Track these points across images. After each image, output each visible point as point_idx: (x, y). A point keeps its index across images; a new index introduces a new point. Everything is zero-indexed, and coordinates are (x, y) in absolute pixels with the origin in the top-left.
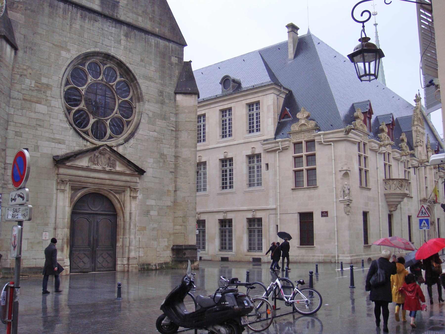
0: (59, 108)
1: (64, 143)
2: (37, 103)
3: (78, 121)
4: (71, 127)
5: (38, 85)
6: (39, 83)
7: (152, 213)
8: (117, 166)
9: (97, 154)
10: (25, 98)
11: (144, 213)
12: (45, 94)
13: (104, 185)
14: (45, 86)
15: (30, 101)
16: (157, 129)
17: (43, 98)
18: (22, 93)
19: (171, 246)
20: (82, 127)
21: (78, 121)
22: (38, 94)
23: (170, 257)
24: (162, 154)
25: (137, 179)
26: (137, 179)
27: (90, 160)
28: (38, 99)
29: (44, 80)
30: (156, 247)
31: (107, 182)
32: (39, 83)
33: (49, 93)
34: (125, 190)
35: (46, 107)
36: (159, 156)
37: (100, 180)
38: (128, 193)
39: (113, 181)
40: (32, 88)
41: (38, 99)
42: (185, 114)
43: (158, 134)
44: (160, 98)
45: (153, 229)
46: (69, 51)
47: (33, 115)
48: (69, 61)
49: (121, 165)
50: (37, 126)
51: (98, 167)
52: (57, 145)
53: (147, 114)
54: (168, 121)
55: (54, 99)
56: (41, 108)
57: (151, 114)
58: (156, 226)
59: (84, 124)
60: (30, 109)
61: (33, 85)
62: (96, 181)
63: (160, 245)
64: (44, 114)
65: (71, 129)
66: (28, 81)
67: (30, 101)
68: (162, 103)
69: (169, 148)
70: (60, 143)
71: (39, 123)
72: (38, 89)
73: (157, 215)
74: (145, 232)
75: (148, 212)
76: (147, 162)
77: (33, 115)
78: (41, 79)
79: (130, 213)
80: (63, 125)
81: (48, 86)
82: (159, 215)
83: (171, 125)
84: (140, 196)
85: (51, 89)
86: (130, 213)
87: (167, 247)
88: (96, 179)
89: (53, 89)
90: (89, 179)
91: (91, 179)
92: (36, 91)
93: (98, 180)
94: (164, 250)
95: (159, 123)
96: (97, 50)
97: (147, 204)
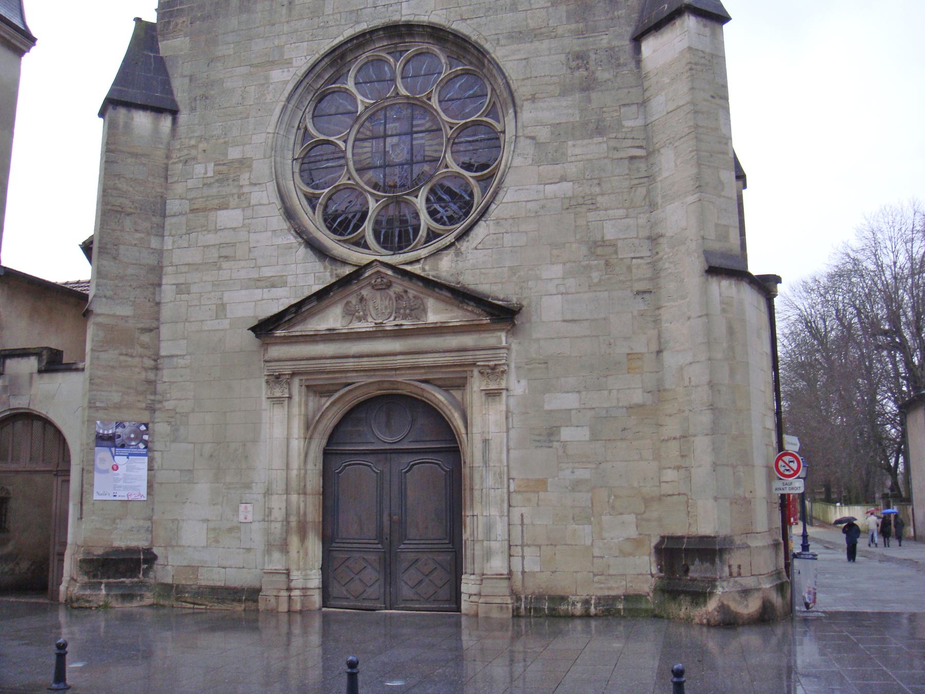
0: (269, 204)
1: (284, 284)
2: (220, 209)
3: (338, 220)
4: (300, 240)
5: (220, 168)
6: (224, 164)
7: (566, 434)
8: (429, 310)
9: (364, 292)
10: (195, 207)
11: (538, 438)
12: (236, 183)
13: (396, 369)
14: (236, 165)
15: (205, 210)
16: (572, 169)
17: (233, 195)
18: (188, 197)
19: (655, 541)
20: (349, 230)
21: (338, 220)
22: (220, 189)
23: (652, 575)
24: (595, 242)
25: (500, 337)
26: (502, 338)
27: (349, 313)
28: (221, 200)
29: (234, 154)
31: (400, 361)
32: (224, 164)
33: (244, 178)
34: (464, 375)
35: (238, 212)
36: (584, 250)
37: (376, 359)
38: (477, 384)
39: (416, 356)
40: (209, 181)
41: (221, 200)
42: (663, 93)
43: (576, 186)
44: (577, 74)
45: (576, 486)
46: (289, 63)
47: (211, 238)
48: (290, 87)
49: (441, 306)
50: (221, 259)
51: (365, 325)
52: (267, 293)
53: (528, 137)
54: (613, 135)
55: (256, 188)
56: (229, 218)
57: (543, 134)
58: (583, 474)
59: (354, 221)
60: (204, 228)
61: (210, 174)
63: (605, 535)
64: (234, 229)
65: (300, 244)
66: (199, 169)
67: (205, 210)
68: (588, 86)
69: (627, 217)
70: (273, 286)
71: (224, 252)
72: (221, 176)
73: (587, 438)
74: (542, 495)
75: (551, 434)
76: (538, 279)
77: (211, 238)
78: (226, 154)
79: (486, 442)
80: (279, 241)
81: (244, 163)
82: (594, 438)
83: (629, 143)
84: (517, 386)
85: (250, 166)
86: (486, 442)
87: (638, 543)
89: (255, 165)
92: (217, 185)
93: (370, 359)
94: (623, 554)
95: (578, 151)
96: (363, 27)
97: (547, 407)
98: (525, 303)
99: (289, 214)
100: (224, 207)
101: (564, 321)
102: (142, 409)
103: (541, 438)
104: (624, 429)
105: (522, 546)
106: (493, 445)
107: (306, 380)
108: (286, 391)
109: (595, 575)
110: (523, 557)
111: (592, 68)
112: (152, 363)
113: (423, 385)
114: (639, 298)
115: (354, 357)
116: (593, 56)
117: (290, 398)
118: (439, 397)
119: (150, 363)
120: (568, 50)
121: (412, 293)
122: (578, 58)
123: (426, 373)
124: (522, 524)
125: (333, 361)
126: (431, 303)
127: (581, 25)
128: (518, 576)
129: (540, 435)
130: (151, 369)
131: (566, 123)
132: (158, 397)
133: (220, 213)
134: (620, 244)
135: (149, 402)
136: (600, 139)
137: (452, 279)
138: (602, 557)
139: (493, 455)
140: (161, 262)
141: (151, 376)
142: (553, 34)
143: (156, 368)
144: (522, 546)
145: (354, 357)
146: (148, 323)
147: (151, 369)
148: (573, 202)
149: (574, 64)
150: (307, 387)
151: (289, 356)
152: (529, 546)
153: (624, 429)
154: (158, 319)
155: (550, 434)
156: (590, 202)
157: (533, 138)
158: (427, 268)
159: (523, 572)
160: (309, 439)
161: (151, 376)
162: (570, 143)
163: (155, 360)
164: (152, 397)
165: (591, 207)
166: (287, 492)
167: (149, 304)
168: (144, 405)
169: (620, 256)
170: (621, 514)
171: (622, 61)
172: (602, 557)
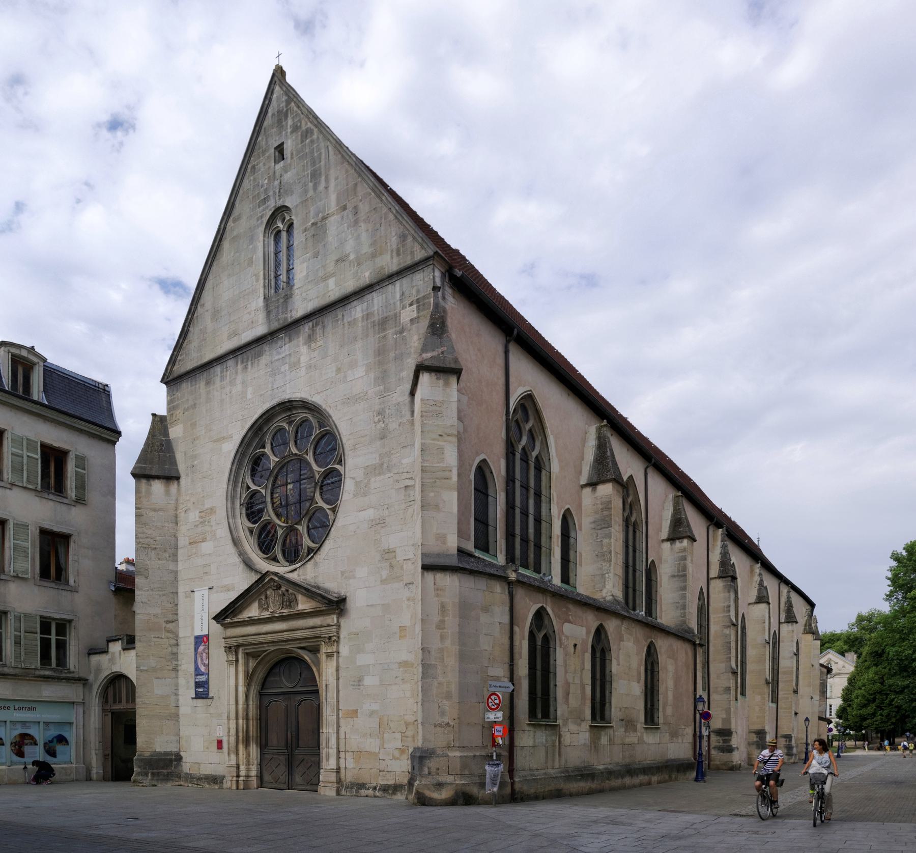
11: (353, 683)
19: (411, 750)
23: (409, 772)
30: (377, 751)
31: (286, 635)
38: (324, 649)
62: (270, 638)
87: (402, 751)
88: (269, 635)
90: (260, 636)
91: (263, 636)
98: (348, 595)
99: (236, 542)
100: (204, 540)
101: (368, 606)
102: (169, 670)
103: (355, 683)
104: (396, 677)
105: (345, 752)
106: (330, 688)
107: (245, 649)
108: (234, 656)
109: (380, 771)
110: (345, 759)
111: (387, 421)
112: (175, 642)
113: (300, 651)
114: (406, 587)
115: (263, 634)
116: (387, 411)
117: (237, 661)
118: (307, 656)
119: (174, 642)
120: (373, 410)
121: (291, 591)
122: (379, 414)
123: (299, 643)
124: (345, 738)
125: (255, 637)
126: (300, 597)
127: (382, 387)
128: (343, 771)
129: (354, 681)
130: (174, 645)
131: (371, 465)
133: (203, 543)
134: (398, 550)
135: (174, 665)
136: (388, 475)
137: (312, 581)
138: (384, 760)
139: (330, 695)
141: (175, 650)
142: (366, 397)
144: (345, 752)
145: (263, 634)
146: (171, 618)
147: (174, 645)
148: (374, 523)
149: (376, 419)
150: (247, 653)
151: (235, 634)
152: (348, 751)
153: (396, 677)
155: (360, 681)
156: (382, 522)
157: (353, 478)
158: (300, 574)
159: (346, 768)
160: (248, 686)
162: (373, 480)
165: (383, 525)
166: (237, 718)
167: (170, 605)
168: (171, 668)
169: (397, 559)
170: (394, 732)
171: (403, 413)
172: (384, 760)
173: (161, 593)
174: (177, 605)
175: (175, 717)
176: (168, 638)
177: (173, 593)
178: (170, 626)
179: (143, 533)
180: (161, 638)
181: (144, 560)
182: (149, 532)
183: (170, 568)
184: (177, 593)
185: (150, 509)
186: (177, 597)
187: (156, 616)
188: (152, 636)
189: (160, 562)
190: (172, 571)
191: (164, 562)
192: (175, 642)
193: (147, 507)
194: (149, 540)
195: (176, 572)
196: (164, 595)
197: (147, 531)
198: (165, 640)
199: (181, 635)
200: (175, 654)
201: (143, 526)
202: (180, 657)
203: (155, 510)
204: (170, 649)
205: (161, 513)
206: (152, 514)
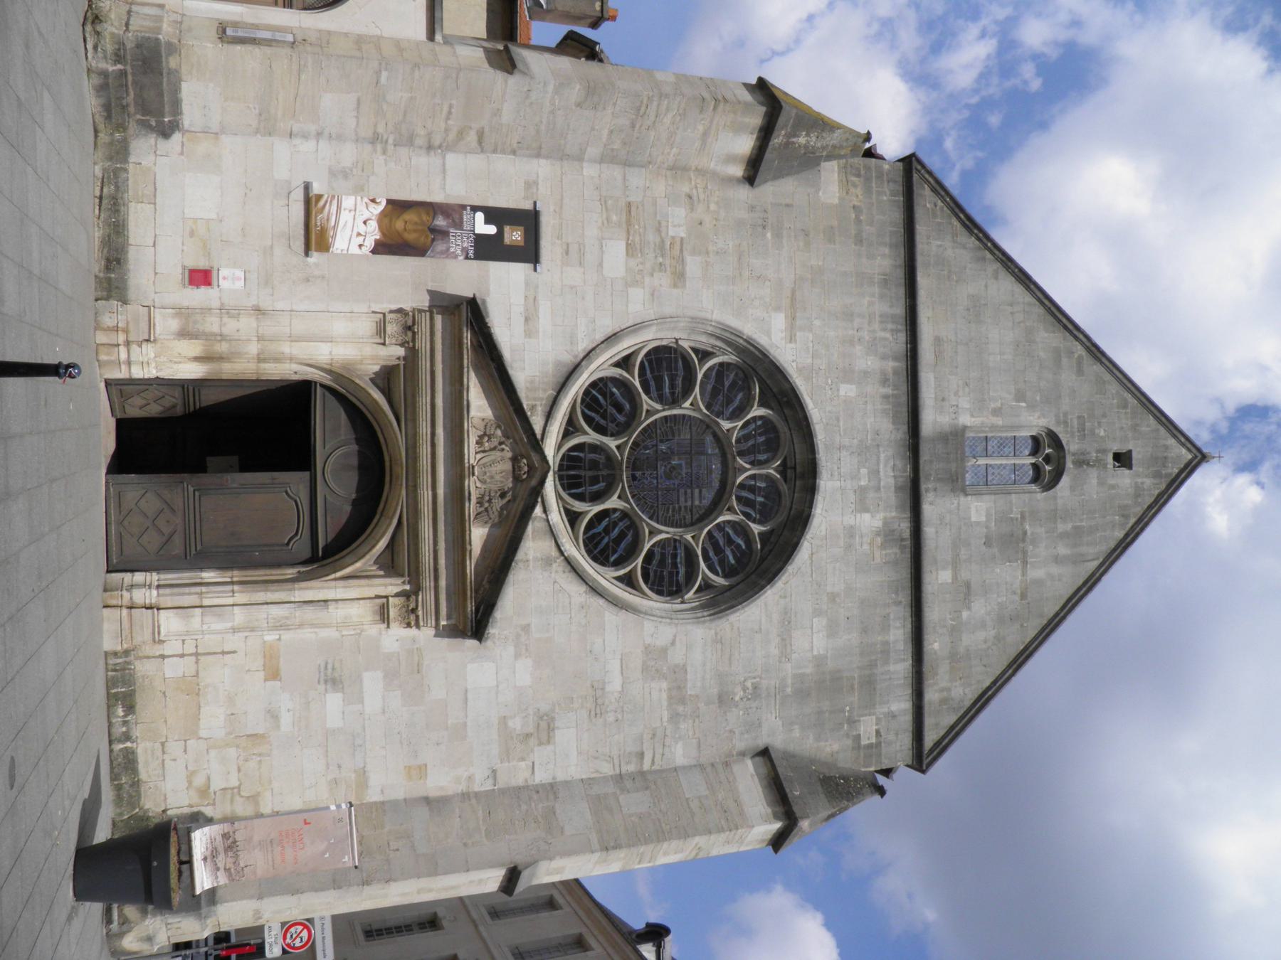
102: (375, 126)
112: (437, 143)
119: (437, 140)
130: (429, 142)
132: (390, 148)
135: (385, 137)
140: (567, 159)
141: (419, 141)
143: (430, 147)
147: (429, 142)
154: (495, 151)
161: (419, 141)
163: (440, 147)
164: (391, 141)
168: (381, 130)
173: (543, 128)
174: (514, 152)
175: (266, 126)
176: (447, 130)
177: (540, 148)
178: (472, 137)
179: (668, 110)
180: (448, 118)
181: (615, 104)
182: (667, 120)
183: (589, 149)
184: (538, 156)
185: (710, 126)
186: (531, 156)
187: (497, 113)
188: (454, 102)
189: (605, 133)
190: (583, 151)
191: (604, 140)
192: (437, 143)
193: (715, 122)
194: (652, 118)
195: (580, 158)
196: (538, 132)
197: (670, 116)
198: (443, 125)
199: (450, 157)
200: (410, 141)
201: (681, 111)
202: (403, 151)
203: (705, 134)
204: (422, 132)
205: (697, 144)
206: (701, 128)
